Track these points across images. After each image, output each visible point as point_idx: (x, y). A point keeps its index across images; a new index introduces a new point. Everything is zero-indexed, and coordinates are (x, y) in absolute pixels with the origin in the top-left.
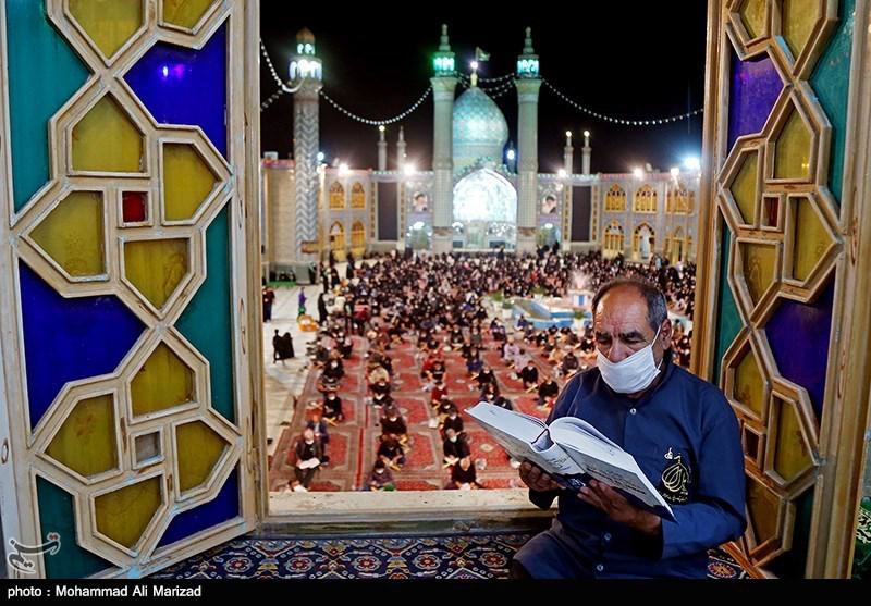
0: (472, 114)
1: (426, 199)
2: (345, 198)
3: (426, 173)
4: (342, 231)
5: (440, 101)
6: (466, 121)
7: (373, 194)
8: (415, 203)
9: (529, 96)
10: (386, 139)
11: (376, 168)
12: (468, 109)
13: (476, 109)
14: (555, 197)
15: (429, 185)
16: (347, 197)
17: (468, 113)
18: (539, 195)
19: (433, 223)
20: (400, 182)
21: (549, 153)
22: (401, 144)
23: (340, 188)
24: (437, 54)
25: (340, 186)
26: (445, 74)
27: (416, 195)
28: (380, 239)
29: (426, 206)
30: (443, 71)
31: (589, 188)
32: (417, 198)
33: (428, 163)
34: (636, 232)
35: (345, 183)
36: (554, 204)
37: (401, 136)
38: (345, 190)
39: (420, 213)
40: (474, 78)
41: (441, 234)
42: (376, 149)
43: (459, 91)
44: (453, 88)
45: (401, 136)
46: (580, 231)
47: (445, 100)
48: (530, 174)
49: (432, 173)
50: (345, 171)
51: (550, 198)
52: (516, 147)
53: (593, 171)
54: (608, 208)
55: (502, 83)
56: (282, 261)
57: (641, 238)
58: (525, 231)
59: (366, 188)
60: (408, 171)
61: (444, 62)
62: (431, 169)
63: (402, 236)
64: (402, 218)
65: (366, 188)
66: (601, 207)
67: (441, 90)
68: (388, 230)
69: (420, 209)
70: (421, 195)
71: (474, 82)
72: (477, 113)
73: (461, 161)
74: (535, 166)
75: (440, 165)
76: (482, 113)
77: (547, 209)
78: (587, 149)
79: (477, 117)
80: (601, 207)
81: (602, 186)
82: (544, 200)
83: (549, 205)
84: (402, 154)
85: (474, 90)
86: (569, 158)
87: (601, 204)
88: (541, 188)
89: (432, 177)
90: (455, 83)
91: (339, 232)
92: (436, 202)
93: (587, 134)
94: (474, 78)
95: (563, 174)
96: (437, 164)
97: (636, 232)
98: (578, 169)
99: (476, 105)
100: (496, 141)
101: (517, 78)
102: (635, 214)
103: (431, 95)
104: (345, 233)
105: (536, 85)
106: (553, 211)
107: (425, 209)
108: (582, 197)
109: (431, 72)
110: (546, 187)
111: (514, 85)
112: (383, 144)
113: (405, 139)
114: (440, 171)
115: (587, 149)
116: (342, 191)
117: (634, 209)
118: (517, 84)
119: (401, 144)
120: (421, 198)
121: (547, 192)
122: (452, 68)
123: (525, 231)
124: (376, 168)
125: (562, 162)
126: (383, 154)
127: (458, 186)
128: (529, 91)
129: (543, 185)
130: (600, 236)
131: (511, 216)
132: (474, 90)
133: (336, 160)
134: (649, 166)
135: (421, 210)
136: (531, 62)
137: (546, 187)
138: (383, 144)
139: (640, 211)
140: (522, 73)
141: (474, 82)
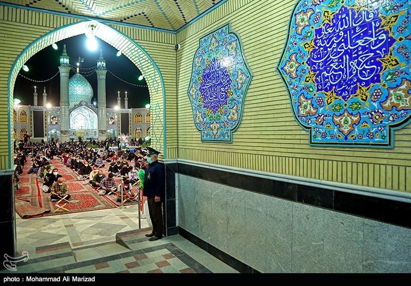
7: (31, 116)
11: (32, 105)
13: (79, 82)
18: (107, 116)
20: (44, 110)
21: (111, 99)
22: (45, 94)
28: (35, 137)
30: (64, 63)
33: (57, 102)
34: (147, 131)
39: (55, 125)
40: (78, 69)
41: (65, 134)
43: (72, 74)
48: (103, 110)
52: (97, 100)
53: (129, 108)
55: (93, 69)
57: (149, 132)
58: (102, 132)
59: (28, 113)
60: (48, 106)
63: (46, 135)
64: (46, 127)
65: (28, 113)
67: (63, 72)
68: (39, 132)
69: (54, 123)
70: (54, 117)
71: (78, 71)
73: (72, 105)
77: (111, 123)
78: (126, 98)
80: (133, 123)
81: (133, 113)
84: (45, 98)
86: (119, 102)
87: (133, 120)
92: (62, 120)
93: (126, 92)
94: (78, 69)
95: (117, 108)
96: (62, 104)
97: (147, 131)
98: (123, 106)
100: (88, 96)
101: (97, 69)
103: (59, 74)
105: (105, 72)
106: (113, 123)
107: (56, 123)
108: (125, 118)
110: (110, 113)
112: (36, 94)
115: (126, 98)
118: (97, 71)
119: (45, 94)
121: (110, 116)
122: (68, 63)
123: (102, 132)
124: (32, 105)
125: (116, 103)
126: (36, 98)
127: (73, 113)
128: (102, 74)
130: (133, 133)
131: (96, 127)
137: (110, 113)
138: (36, 94)
141: (78, 71)
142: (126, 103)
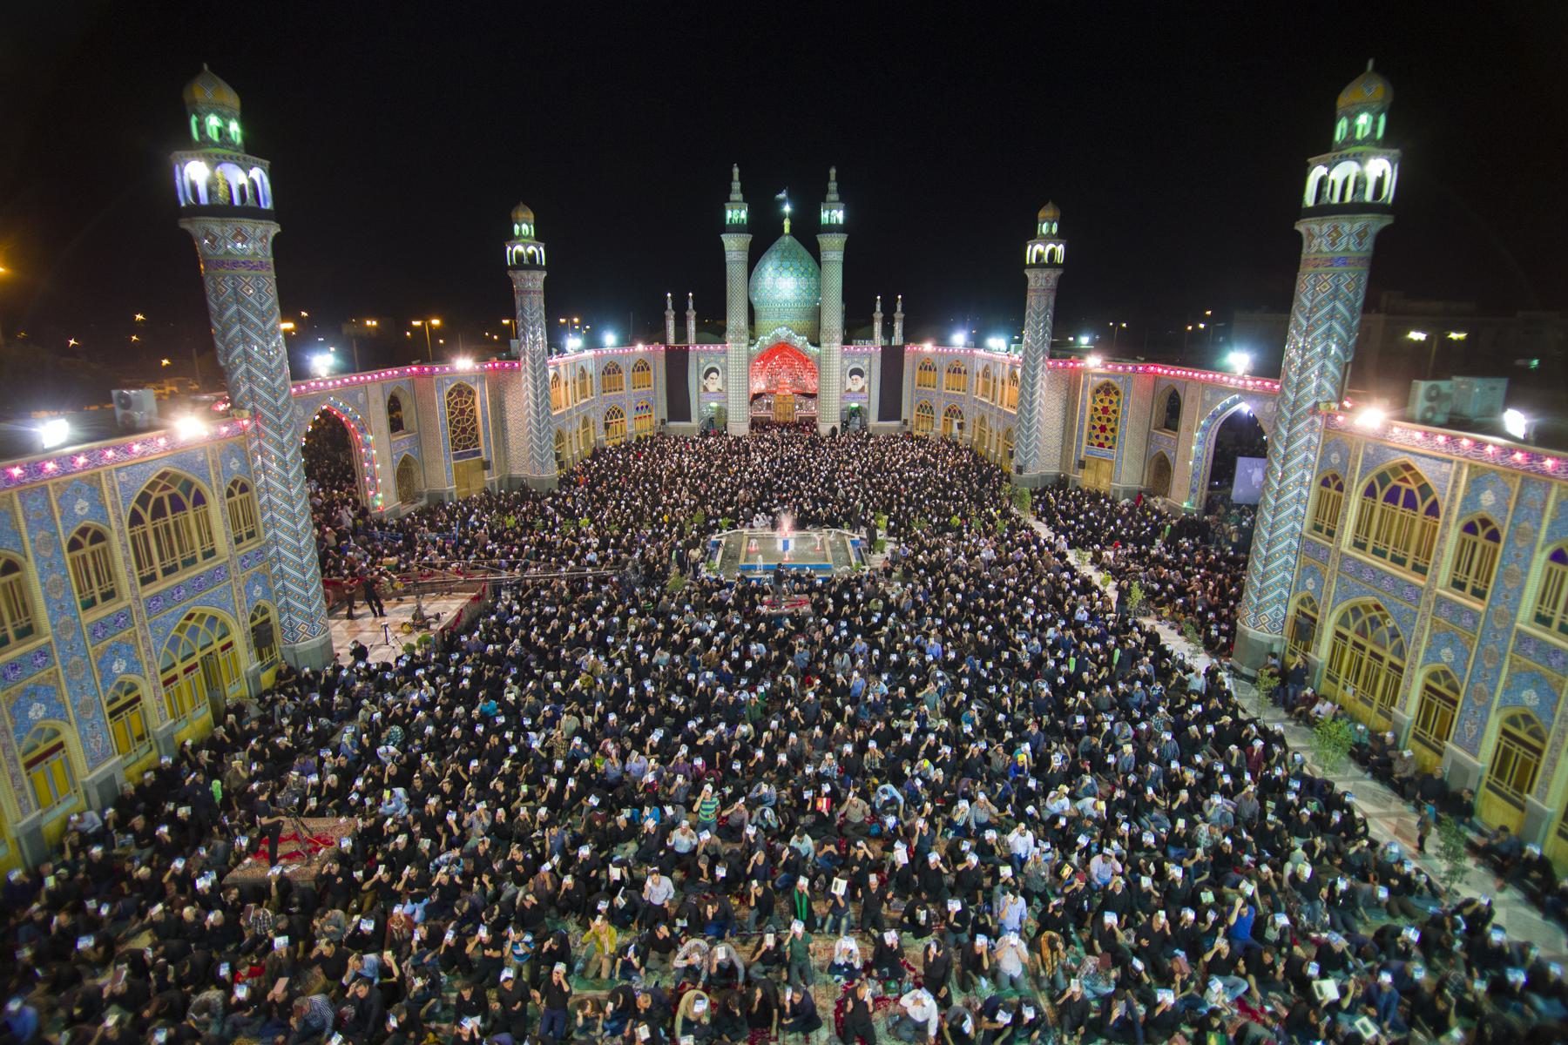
9: (833, 249)
12: (776, 263)
40: (787, 223)
42: (663, 319)
46: (890, 409)
56: (515, 473)
61: (736, 214)
67: (735, 247)
71: (787, 230)
74: (838, 337)
85: (787, 240)
94: (787, 223)
115: (899, 315)
120: (713, 375)
132: (787, 240)
141: (787, 230)
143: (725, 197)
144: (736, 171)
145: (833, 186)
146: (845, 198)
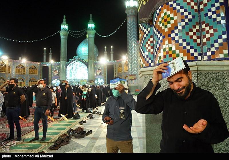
0: (83, 45)
1: (58, 72)
2: (26, 71)
3: (57, 62)
4: (24, 81)
5: (62, 39)
6: (81, 48)
8: (54, 73)
10: (46, 52)
13: (85, 44)
14: (101, 69)
15: (59, 67)
16: (27, 70)
17: (82, 45)
18: (95, 68)
19: (60, 79)
22: (51, 54)
23: (23, 67)
24: (62, 24)
25: (23, 66)
26: (63, 30)
27: (54, 70)
29: (58, 73)
31: (113, 65)
32: (55, 71)
35: (25, 66)
36: (100, 71)
37: (51, 51)
38: (26, 68)
39: (56, 76)
44: (67, 35)
45: (51, 51)
47: (63, 38)
49: (59, 62)
50: (24, 61)
51: (99, 69)
53: (114, 60)
54: (119, 72)
60: (52, 61)
61: (64, 27)
62: (60, 61)
63: (50, 84)
64: (50, 77)
66: (117, 72)
69: (56, 74)
72: (85, 45)
75: (61, 60)
76: (86, 45)
77: (98, 73)
78: (112, 52)
79: (85, 46)
80: (117, 72)
82: (97, 71)
83: (99, 72)
84: (50, 57)
88: (96, 66)
89: (60, 64)
90: (68, 34)
91: (22, 82)
96: (61, 60)
99: (85, 43)
102: (124, 72)
104: (25, 82)
106: (100, 74)
107: (57, 74)
109: (60, 29)
111: (86, 32)
112: (45, 54)
113: (52, 52)
114: (62, 62)
115: (112, 52)
116: (24, 68)
117: (124, 71)
119: (51, 54)
120: (56, 71)
126: (45, 57)
129: (97, 65)
133: (20, 58)
134: (126, 54)
135: (56, 75)
136: (91, 24)
139: (126, 71)
140: (88, 28)
142: (112, 55)
143: (61, 22)
144: (64, 16)
145: (91, 18)
146: (95, 21)
